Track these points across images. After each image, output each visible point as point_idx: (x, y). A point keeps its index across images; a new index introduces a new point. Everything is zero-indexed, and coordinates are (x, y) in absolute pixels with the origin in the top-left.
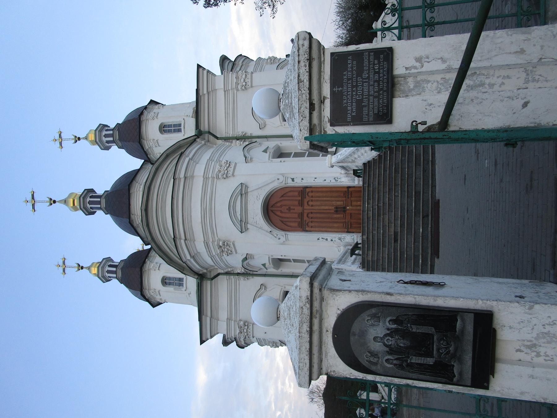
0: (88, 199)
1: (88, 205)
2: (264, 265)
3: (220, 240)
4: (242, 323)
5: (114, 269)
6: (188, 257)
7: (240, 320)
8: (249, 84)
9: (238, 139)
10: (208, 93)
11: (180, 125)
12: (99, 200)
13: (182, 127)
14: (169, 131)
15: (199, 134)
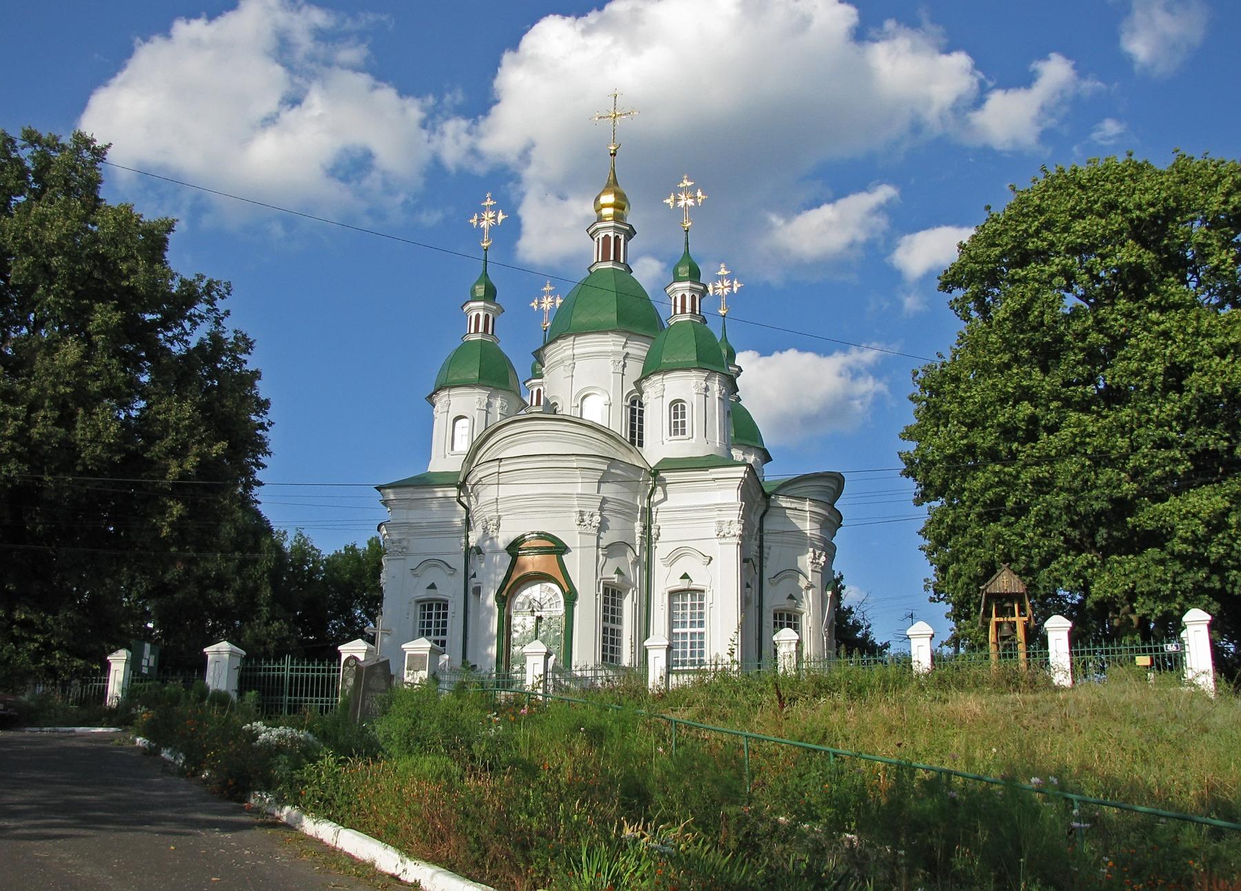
0: (611, 234)
1: (603, 235)
2: (474, 576)
3: (499, 517)
4: (405, 543)
5: (481, 329)
6: (480, 475)
7: (409, 541)
8: (723, 540)
9: (645, 528)
10: (714, 479)
11: (683, 433)
12: (612, 258)
13: (680, 436)
14: (676, 416)
15: (655, 473)
